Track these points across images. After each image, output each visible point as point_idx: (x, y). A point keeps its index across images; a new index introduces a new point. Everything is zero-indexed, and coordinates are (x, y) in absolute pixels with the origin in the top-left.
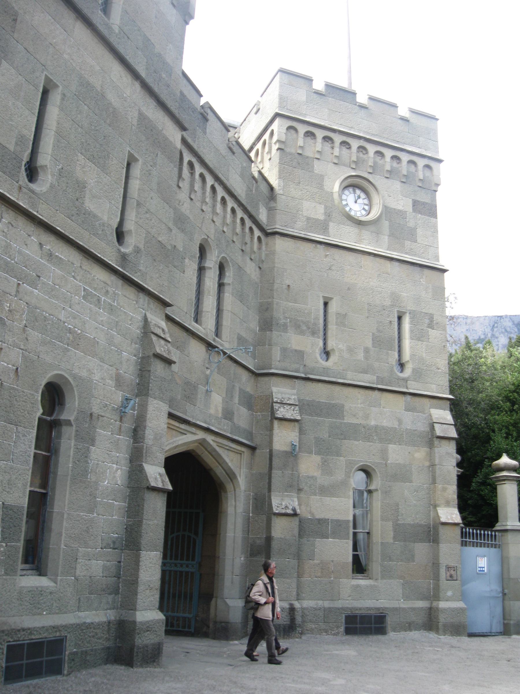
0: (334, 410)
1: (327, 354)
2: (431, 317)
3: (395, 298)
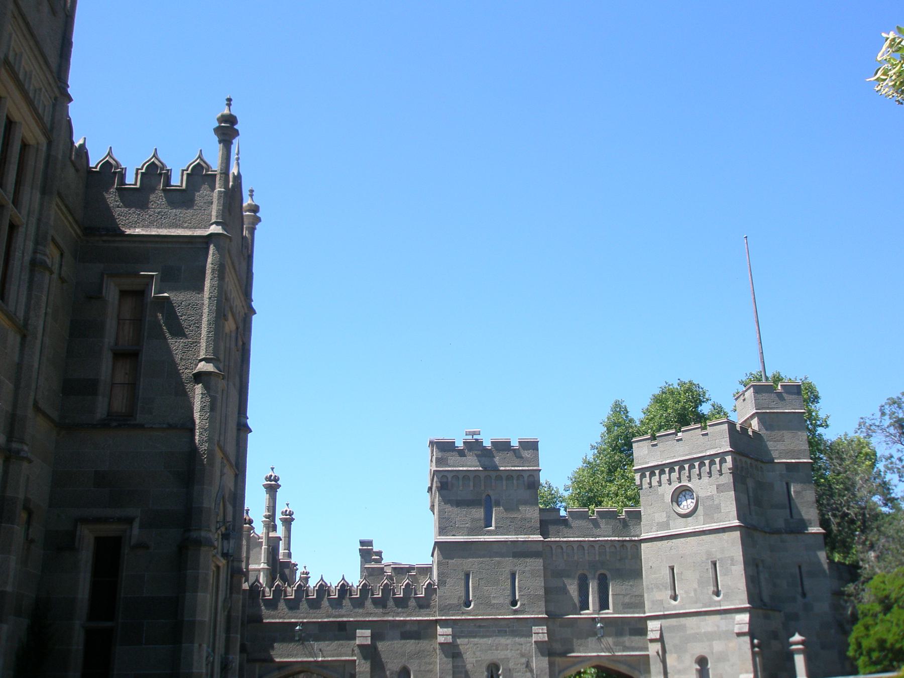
0: (683, 628)
1: (675, 598)
2: (732, 559)
3: (709, 553)
